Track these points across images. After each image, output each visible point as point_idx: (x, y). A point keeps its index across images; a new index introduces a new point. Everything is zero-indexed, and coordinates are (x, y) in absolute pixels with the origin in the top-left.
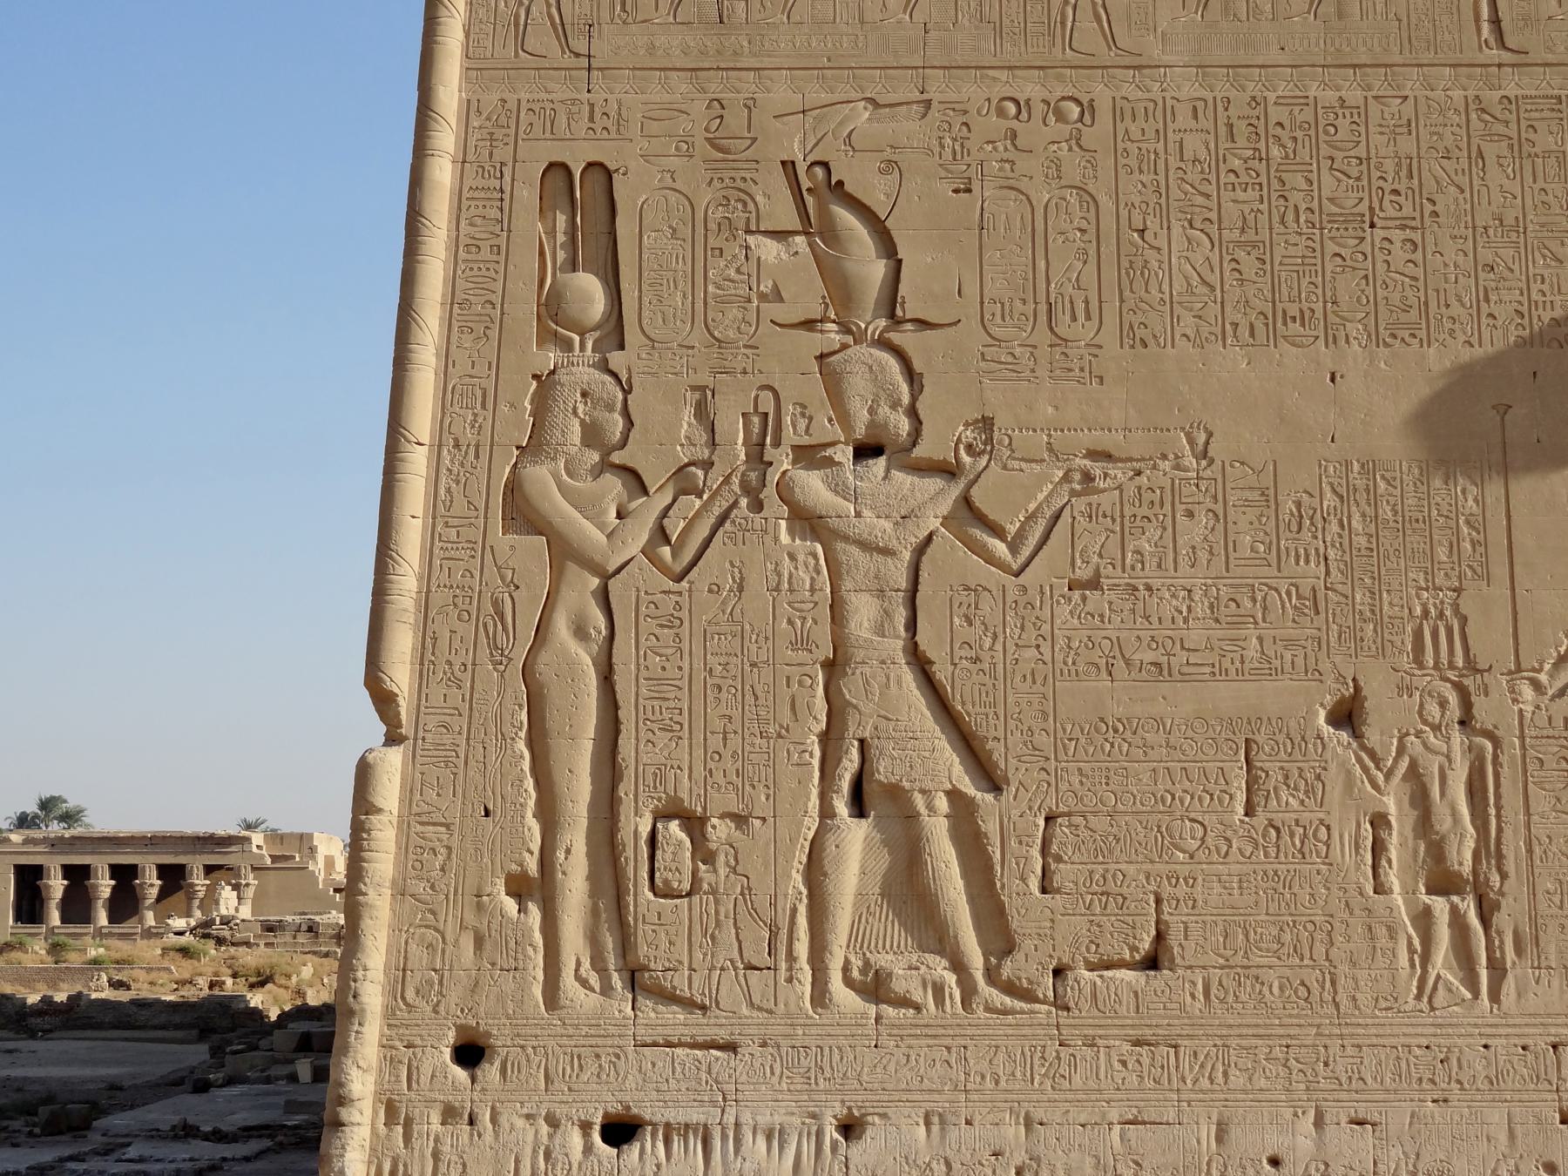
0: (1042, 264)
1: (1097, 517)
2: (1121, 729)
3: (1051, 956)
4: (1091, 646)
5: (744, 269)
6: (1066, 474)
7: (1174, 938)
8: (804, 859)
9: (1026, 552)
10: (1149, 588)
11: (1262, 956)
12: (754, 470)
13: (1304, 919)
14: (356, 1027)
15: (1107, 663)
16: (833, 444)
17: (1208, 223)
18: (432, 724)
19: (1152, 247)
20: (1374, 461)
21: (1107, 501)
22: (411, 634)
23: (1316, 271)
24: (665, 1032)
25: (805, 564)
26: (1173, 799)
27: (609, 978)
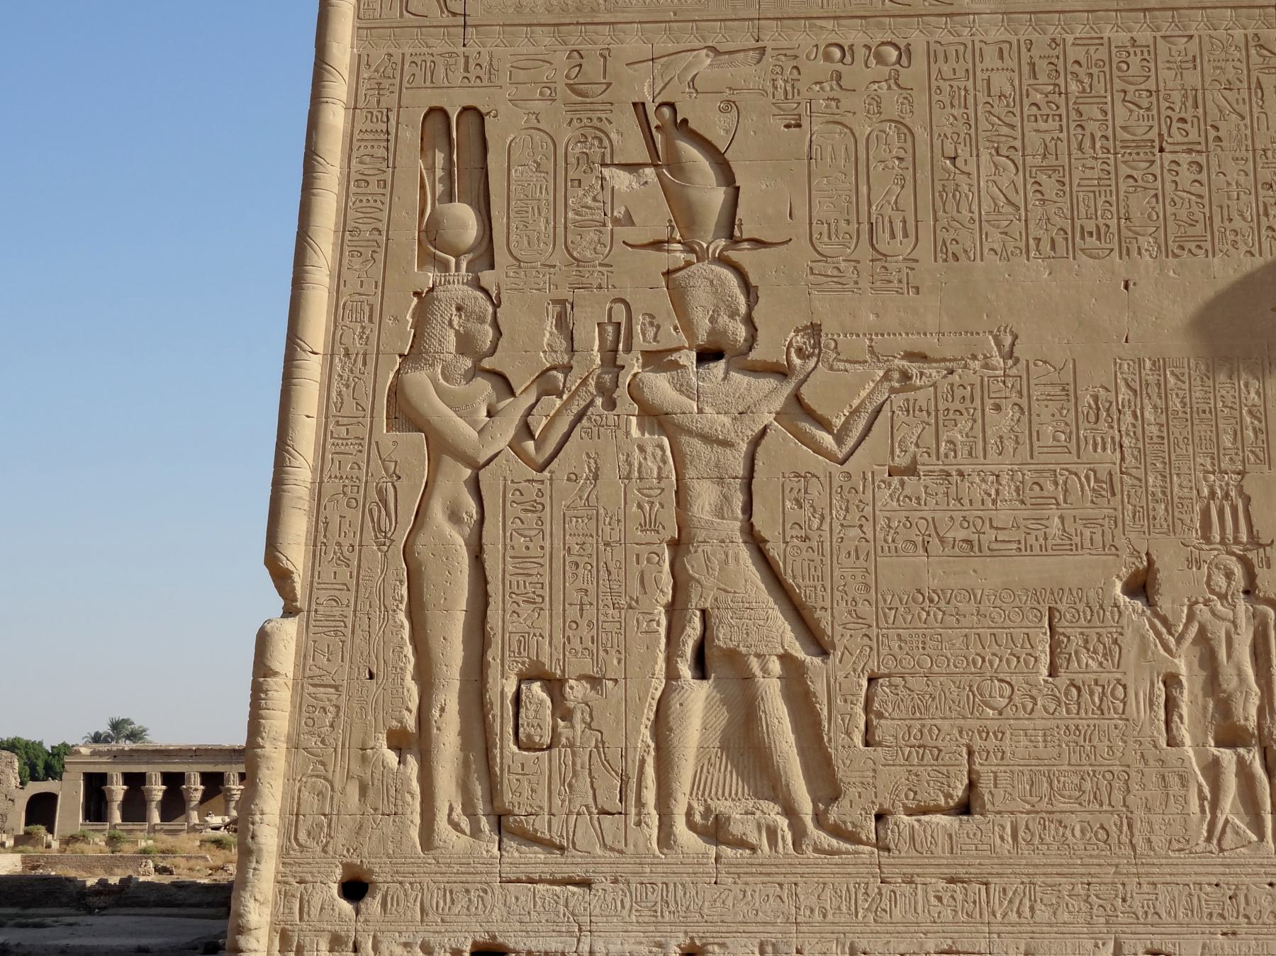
0: (863, 189)
1: (914, 411)
2: (936, 599)
3: (873, 802)
4: (909, 525)
5: (600, 197)
6: (886, 373)
7: (985, 786)
8: (652, 716)
9: (850, 442)
10: (961, 474)
11: (1065, 803)
12: (608, 373)
13: (1103, 768)
14: (254, 865)
15: (923, 541)
16: (678, 349)
17: (1012, 150)
18: (323, 596)
19: (963, 173)
20: (1164, 359)
21: (923, 397)
22: (306, 518)
23: (1111, 191)
24: (527, 870)
25: (653, 455)
26: (984, 661)
27: (478, 822)
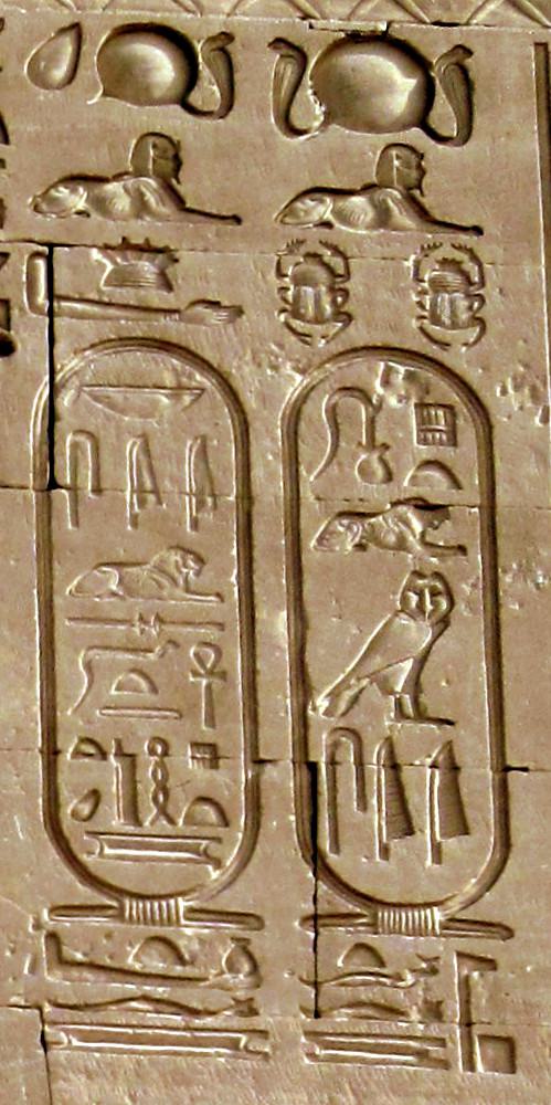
0: (277, 624)
